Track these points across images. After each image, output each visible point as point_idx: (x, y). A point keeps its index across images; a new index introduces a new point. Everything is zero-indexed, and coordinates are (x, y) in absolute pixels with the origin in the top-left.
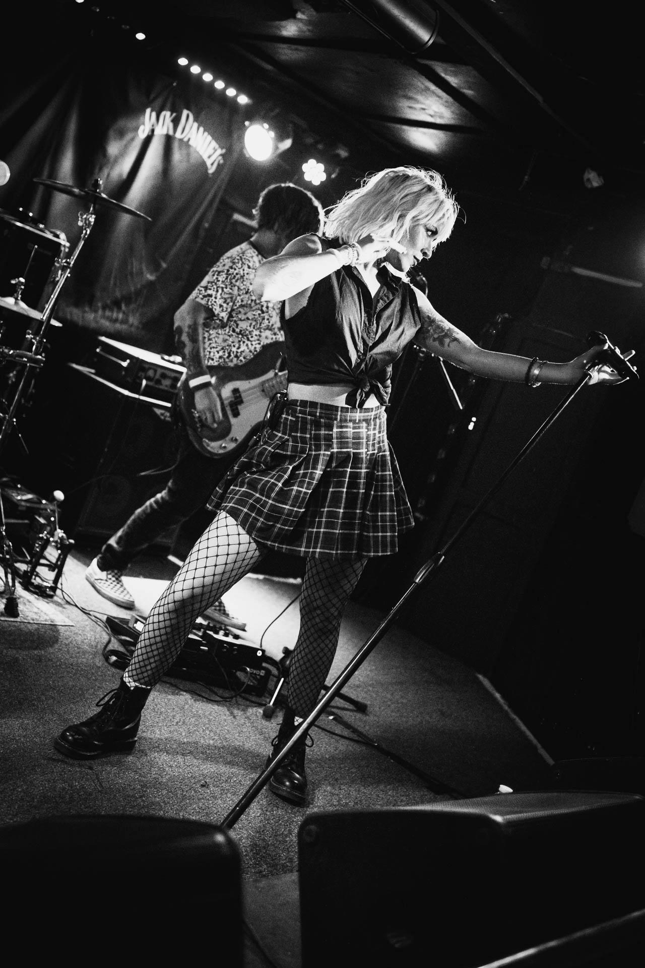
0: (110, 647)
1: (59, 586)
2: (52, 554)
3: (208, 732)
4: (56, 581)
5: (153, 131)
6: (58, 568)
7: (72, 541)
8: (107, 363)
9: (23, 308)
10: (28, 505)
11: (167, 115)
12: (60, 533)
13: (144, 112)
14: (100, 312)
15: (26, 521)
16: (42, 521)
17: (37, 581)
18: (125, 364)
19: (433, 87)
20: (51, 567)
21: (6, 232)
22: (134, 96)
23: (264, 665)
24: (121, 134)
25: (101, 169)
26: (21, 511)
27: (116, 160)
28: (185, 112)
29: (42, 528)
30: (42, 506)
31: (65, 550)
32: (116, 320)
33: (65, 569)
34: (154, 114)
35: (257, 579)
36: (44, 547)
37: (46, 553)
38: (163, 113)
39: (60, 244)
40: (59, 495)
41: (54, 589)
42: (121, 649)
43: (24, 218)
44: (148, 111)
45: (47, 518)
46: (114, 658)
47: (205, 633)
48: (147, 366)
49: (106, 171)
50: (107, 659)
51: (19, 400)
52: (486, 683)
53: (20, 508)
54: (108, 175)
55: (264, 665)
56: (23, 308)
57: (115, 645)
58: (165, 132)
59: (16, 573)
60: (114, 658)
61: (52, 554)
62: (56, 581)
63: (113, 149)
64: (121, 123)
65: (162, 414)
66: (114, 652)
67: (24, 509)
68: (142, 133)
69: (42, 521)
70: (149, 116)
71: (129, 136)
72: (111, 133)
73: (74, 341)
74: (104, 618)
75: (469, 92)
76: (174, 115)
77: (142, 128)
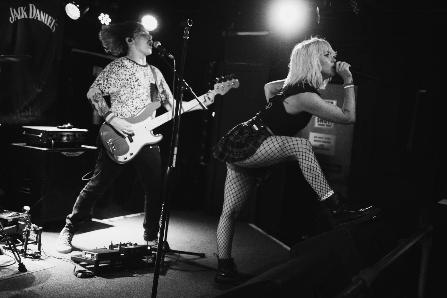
0: (77, 270)
1: (41, 250)
2: (33, 236)
3: (136, 291)
4: (39, 249)
6: (38, 242)
7: (41, 228)
8: (31, 138)
10: (13, 218)
12: (33, 225)
14: (19, 114)
15: (15, 226)
16: (23, 223)
17: (29, 252)
20: (35, 243)
23: (153, 252)
26: (10, 222)
29: (24, 226)
30: (20, 216)
31: (38, 233)
32: (29, 116)
33: (42, 242)
35: (138, 216)
36: (28, 235)
37: (30, 237)
40: (27, 208)
41: (40, 253)
42: (83, 269)
45: (24, 221)
46: (80, 274)
47: (120, 248)
48: (51, 134)
50: (76, 276)
52: (254, 226)
53: (9, 221)
55: (153, 252)
57: (79, 268)
59: (18, 252)
60: (80, 274)
61: (33, 236)
62: (39, 249)
65: (67, 154)
66: (79, 271)
67: (11, 220)
69: (23, 223)
74: (70, 258)
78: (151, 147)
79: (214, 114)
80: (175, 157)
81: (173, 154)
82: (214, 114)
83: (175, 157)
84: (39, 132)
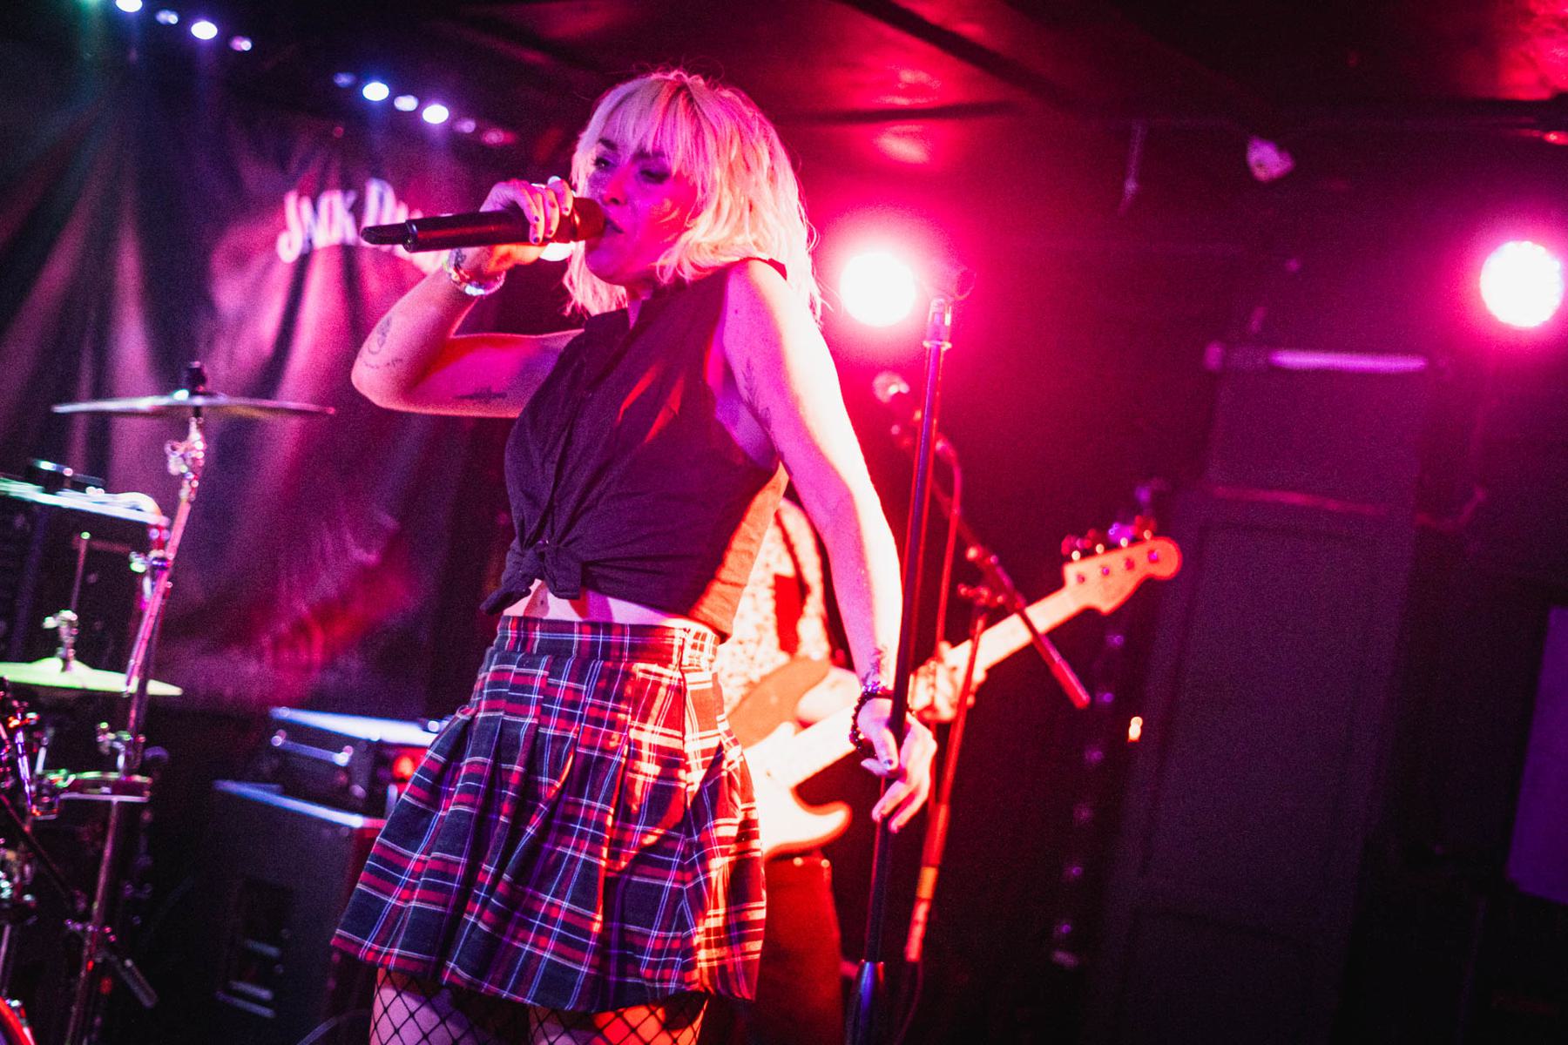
5: (310, 241)
9: (84, 677)
11: (335, 203)
13: (278, 206)
18: (342, 758)
19: (889, 32)
21: (19, 521)
22: (254, 175)
24: (241, 259)
25: (211, 343)
27: (242, 320)
28: (374, 189)
34: (306, 206)
38: (324, 202)
39: (143, 527)
43: (52, 483)
44: (291, 201)
49: (223, 346)
51: (113, 887)
54: (231, 354)
56: (84, 677)
58: (335, 237)
63: (229, 295)
64: (236, 237)
68: (288, 249)
70: (295, 210)
71: (259, 261)
72: (219, 261)
73: (202, 742)
75: (970, 30)
76: (351, 198)
77: (283, 241)
78: (798, 861)
79: (1135, 729)
80: (921, 912)
81: (912, 900)
82: (1135, 729)
83: (921, 912)
84: (337, 741)
